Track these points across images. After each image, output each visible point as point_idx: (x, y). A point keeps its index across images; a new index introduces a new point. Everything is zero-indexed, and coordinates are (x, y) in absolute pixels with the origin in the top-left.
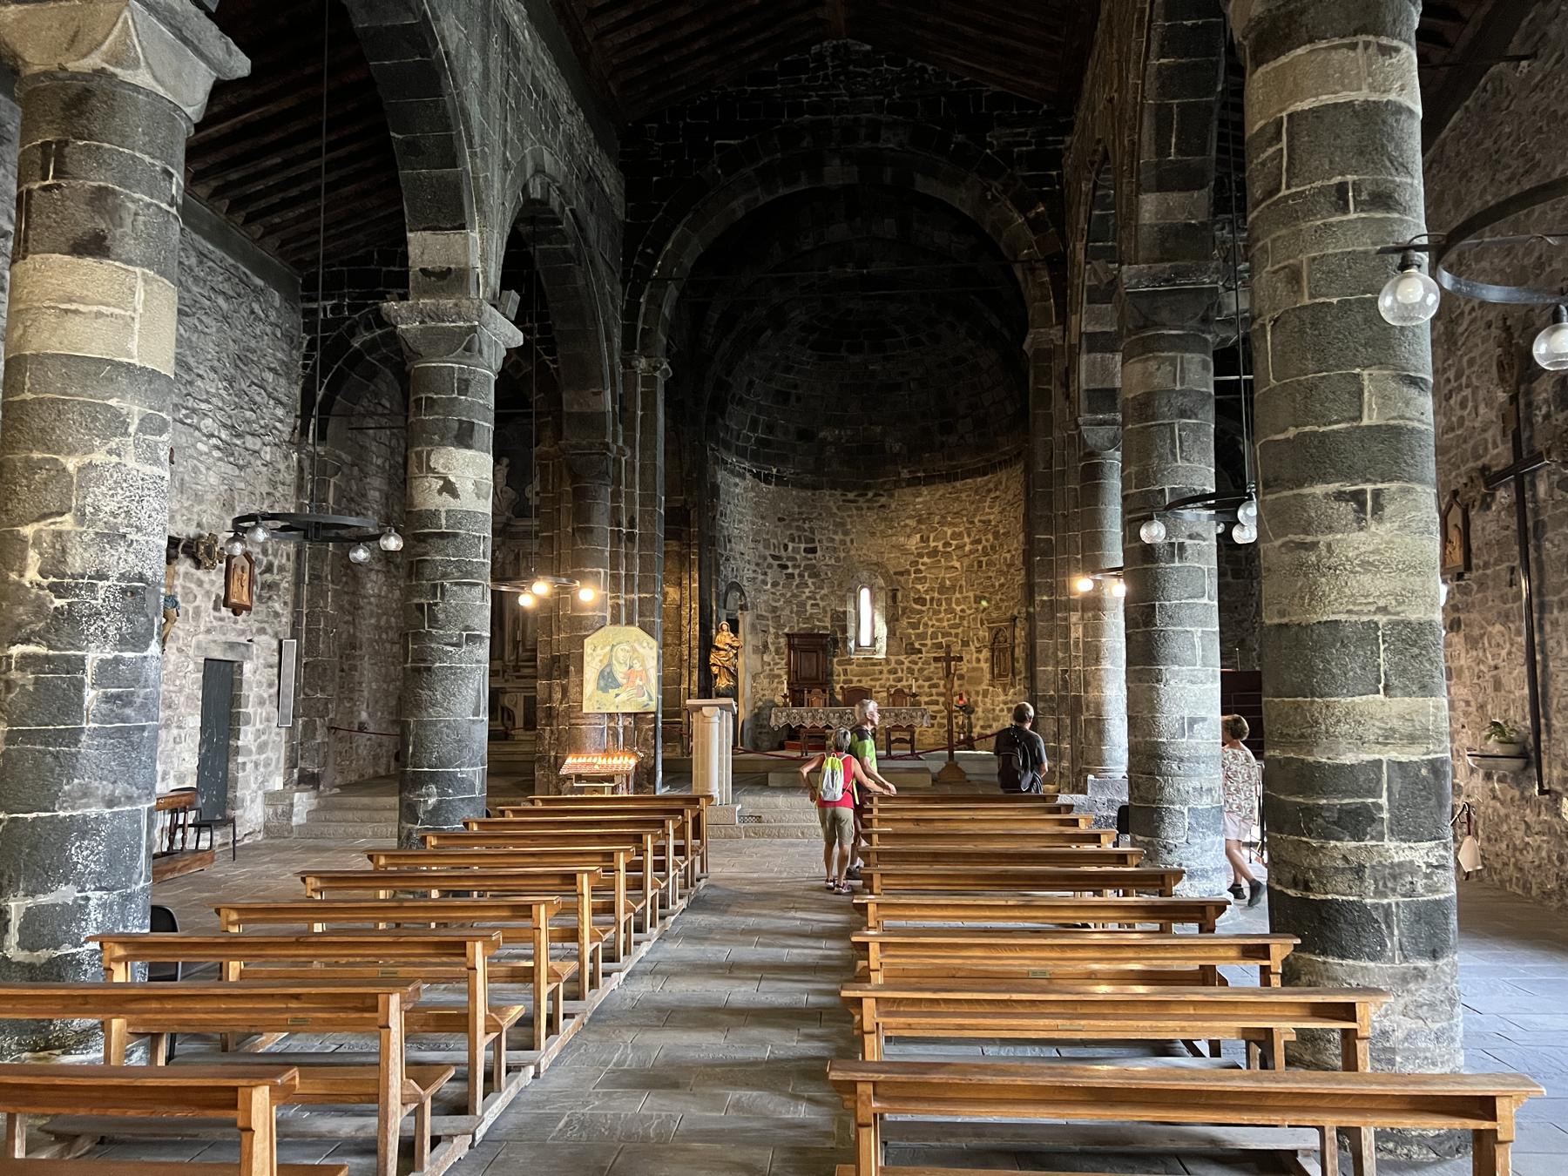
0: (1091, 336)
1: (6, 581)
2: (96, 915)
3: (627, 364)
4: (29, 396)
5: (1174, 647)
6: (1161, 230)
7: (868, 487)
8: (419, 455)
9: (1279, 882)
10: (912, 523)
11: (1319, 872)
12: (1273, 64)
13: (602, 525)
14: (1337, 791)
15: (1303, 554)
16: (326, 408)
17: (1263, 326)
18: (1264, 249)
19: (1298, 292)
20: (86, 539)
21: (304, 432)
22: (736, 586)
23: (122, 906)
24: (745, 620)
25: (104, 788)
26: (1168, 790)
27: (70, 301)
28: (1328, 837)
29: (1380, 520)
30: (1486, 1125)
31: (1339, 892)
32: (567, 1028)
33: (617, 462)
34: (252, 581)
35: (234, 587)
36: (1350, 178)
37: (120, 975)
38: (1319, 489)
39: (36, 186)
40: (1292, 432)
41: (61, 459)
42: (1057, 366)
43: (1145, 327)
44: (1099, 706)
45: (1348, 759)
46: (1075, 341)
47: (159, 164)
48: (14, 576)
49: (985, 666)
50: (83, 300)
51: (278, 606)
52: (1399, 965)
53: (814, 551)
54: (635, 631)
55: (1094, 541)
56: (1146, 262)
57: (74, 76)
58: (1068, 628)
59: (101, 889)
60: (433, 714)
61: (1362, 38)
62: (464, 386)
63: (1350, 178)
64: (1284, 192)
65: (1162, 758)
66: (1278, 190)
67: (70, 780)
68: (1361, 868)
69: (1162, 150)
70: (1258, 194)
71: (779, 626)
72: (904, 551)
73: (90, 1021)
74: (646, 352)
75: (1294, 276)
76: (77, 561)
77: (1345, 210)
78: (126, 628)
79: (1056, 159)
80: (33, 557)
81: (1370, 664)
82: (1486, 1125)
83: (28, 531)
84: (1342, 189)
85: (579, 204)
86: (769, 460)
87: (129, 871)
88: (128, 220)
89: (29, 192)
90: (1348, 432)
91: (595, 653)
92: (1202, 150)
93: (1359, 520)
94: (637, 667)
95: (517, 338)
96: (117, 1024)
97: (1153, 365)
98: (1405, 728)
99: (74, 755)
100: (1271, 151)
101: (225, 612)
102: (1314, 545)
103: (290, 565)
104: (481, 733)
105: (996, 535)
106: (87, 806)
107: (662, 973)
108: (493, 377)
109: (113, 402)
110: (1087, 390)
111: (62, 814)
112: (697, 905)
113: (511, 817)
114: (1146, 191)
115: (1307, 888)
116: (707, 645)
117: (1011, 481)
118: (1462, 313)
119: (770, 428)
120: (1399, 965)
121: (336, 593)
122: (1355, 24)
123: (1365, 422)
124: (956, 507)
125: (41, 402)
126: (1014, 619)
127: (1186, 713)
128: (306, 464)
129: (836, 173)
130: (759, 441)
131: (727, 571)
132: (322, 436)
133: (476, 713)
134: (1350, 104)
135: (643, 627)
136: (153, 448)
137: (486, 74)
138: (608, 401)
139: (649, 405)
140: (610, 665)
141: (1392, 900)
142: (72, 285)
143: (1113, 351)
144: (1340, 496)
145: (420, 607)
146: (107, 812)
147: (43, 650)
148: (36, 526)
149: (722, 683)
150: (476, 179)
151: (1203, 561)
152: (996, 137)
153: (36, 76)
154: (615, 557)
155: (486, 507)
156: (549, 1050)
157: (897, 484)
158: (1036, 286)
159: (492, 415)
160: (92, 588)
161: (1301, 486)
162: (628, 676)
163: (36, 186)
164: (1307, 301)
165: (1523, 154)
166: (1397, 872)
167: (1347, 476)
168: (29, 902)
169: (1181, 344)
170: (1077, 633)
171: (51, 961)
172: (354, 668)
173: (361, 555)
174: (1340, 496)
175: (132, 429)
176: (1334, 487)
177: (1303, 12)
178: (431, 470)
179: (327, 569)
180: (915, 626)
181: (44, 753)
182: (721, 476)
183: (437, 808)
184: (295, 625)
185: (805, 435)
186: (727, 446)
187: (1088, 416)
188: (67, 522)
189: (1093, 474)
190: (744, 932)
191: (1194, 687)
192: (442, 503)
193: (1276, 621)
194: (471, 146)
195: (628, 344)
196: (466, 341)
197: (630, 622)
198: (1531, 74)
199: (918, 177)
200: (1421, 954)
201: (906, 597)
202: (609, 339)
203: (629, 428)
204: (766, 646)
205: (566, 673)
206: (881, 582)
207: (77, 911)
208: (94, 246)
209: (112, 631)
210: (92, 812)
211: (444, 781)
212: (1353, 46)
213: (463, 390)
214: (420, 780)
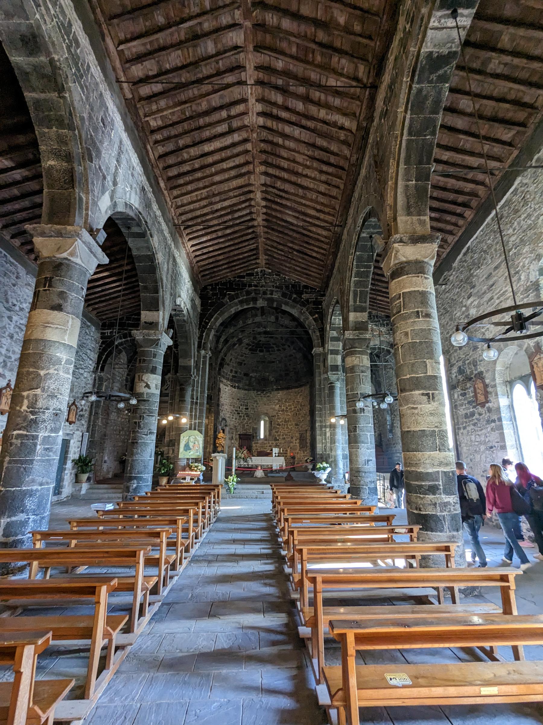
0: (331, 350)
1: (15, 410)
2: (31, 524)
3: (198, 351)
4: (31, 351)
5: (362, 439)
6: (355, 322)
7: (264, 390)
8: (139, 376)
9: (411, 508)
10: (277, 401)
11: (424, 505)
13: (188, 399)
15: (413, 410)
16: (105, 361)
18: (397, 327)
19: (408, 338)
20: (44, 397)
21: (97, 368)
22: (224, 419)
23: (41, 521)
24: (227, 429)
25: (40, 479)
26: (362, 482)
27: (48, 323)
28: (426, 494)
29: (434, 401)
30: (506, 584)
31: (430, 511)
32: (185, 562)
33: (194, 380)
34: (76, 414)
35: (71, 416)
36: (419, 309)
37: (38, 545)
38: (417, 392)
39: (41, 289)
40: (408, 376)
41: (39, 371)
45: (430, 471)
47: (80, 286)
48: (18, 408)
49: (298, 445)
50: (52, 323)
51: (83, 422)
52: (448, 534)
53: (247, 409)
54: (196, 432)
55: (333, 408)
57: (58, 258)
58: (326, 433)
59: (34, 515)
60: (137, 457)
61: (420, 275)
62: (155, 356)
63: (419, 309)
64: (402, 312)
67: (28, 476)
68: (436, 503)
69: (355, 301)
71: (237, 432)
72: (274, 409)
73: (25, 563)
74: (204, 348)
75: (406, 334)
76: (40, 404)
77: (419, 317)
78: (53, 425)
79: (320, 303)
80: (26, 402)
81: (434, 442)
82: (506, 584)
83: (25, 394)
85: (189, 306)
86: (235, 381)
87: (44, 508)
88: (69, 301)
89: (39, 291)
90: (424, 377)
91: (184, 439)
92: (365, 302)
93: (429, 401)
94: (196, 443)
95: (171, 343)
96: (35, 563)
97: (354, 358)
98: (445, 461)
99: (31, 468)
101: (67, 424)
102: (416, 408)
103: (88, 409)
104: (151, 464)
105: (301, 405)
106: (33, 486)
107: (212, 543)
108: (163, 353)
109: (58, 354)
111: (24, 488)
112: (218, 520)
113: (159, 491)
115: (420, 510)
116: (216, 437)
117: (305, 390)
119: (236, 372)
120: (448, 534)
121: (102, 419)
122: (418, 271)
123: (428, 374)
124: (290, 397)
125: (35, 353)
126: (306, 431)
127: (366, 458)
128: (97, 378)
129: (261, 303)
130: (233, 376)
131: (221, 414)
132: (102, 370)
133: (151, 457)
134: (418, 291)
135: (199, 431)
136: (68, 369)
137: (168, 269)
138: (192, 363)
139: (204, 363)
140: (188, 442)
141: (445, 513)
142: (49, 319)
143: (337, 355)
144: (423, 394)
145: (135, 423)
146: (39, 488)
147: (25, 433)
148: (28, 392)
149: (220, 449)
150: (163, 297)
151: (369, 414)
152: (305, 296)
153: (46, 258)
154: (191, 408)
155: (158, 392)
156: (180, 569)
157: (273, 390)
158: (315, 336)
159: (162, 365)
160: (44, 412)
161: (411, 391)
162: (193, 447)
163: (41, 289)
164: (410, 341)
165: (444, 309)
166: (446, 504)
167: (424, 388)
168: (9, 520)
170: (328, 434)
171: (14, 541)
172: (105, 442)
173: (122, 405)
174: (423, 394)
175: (63, 363)
176: (421, 392)
177: (405, 267)
178: (142, 380)
179: (100, 411)
180: (277, 432)
181: (20, 467)
182: (222, 386)
183: (136, 488)
184: (88, 428)
185: (246, 375)
186: (224, 377)
188: (38, 391)
189: (332, 388)
190: (235, 529)
192: (145, 390)
193: (406, 430)
194: (162, 288)
195: (199, 347)
196: (156, 342)
197: (195, 429)
198: (445, 289)
199: (283, 305)
200: (454, 530)
201: (274, 423)
202: (194, 345)
203: (198, 370)
204: (232, 438)
205: (174, 445)
206: (267, 419)
207: (24, 523)
208: (58, 308)
209: (49, 427)
210: (35, 488)
211: (139, 479)
212: (418, 277)
213: (154, 357)
214: (131, 479)
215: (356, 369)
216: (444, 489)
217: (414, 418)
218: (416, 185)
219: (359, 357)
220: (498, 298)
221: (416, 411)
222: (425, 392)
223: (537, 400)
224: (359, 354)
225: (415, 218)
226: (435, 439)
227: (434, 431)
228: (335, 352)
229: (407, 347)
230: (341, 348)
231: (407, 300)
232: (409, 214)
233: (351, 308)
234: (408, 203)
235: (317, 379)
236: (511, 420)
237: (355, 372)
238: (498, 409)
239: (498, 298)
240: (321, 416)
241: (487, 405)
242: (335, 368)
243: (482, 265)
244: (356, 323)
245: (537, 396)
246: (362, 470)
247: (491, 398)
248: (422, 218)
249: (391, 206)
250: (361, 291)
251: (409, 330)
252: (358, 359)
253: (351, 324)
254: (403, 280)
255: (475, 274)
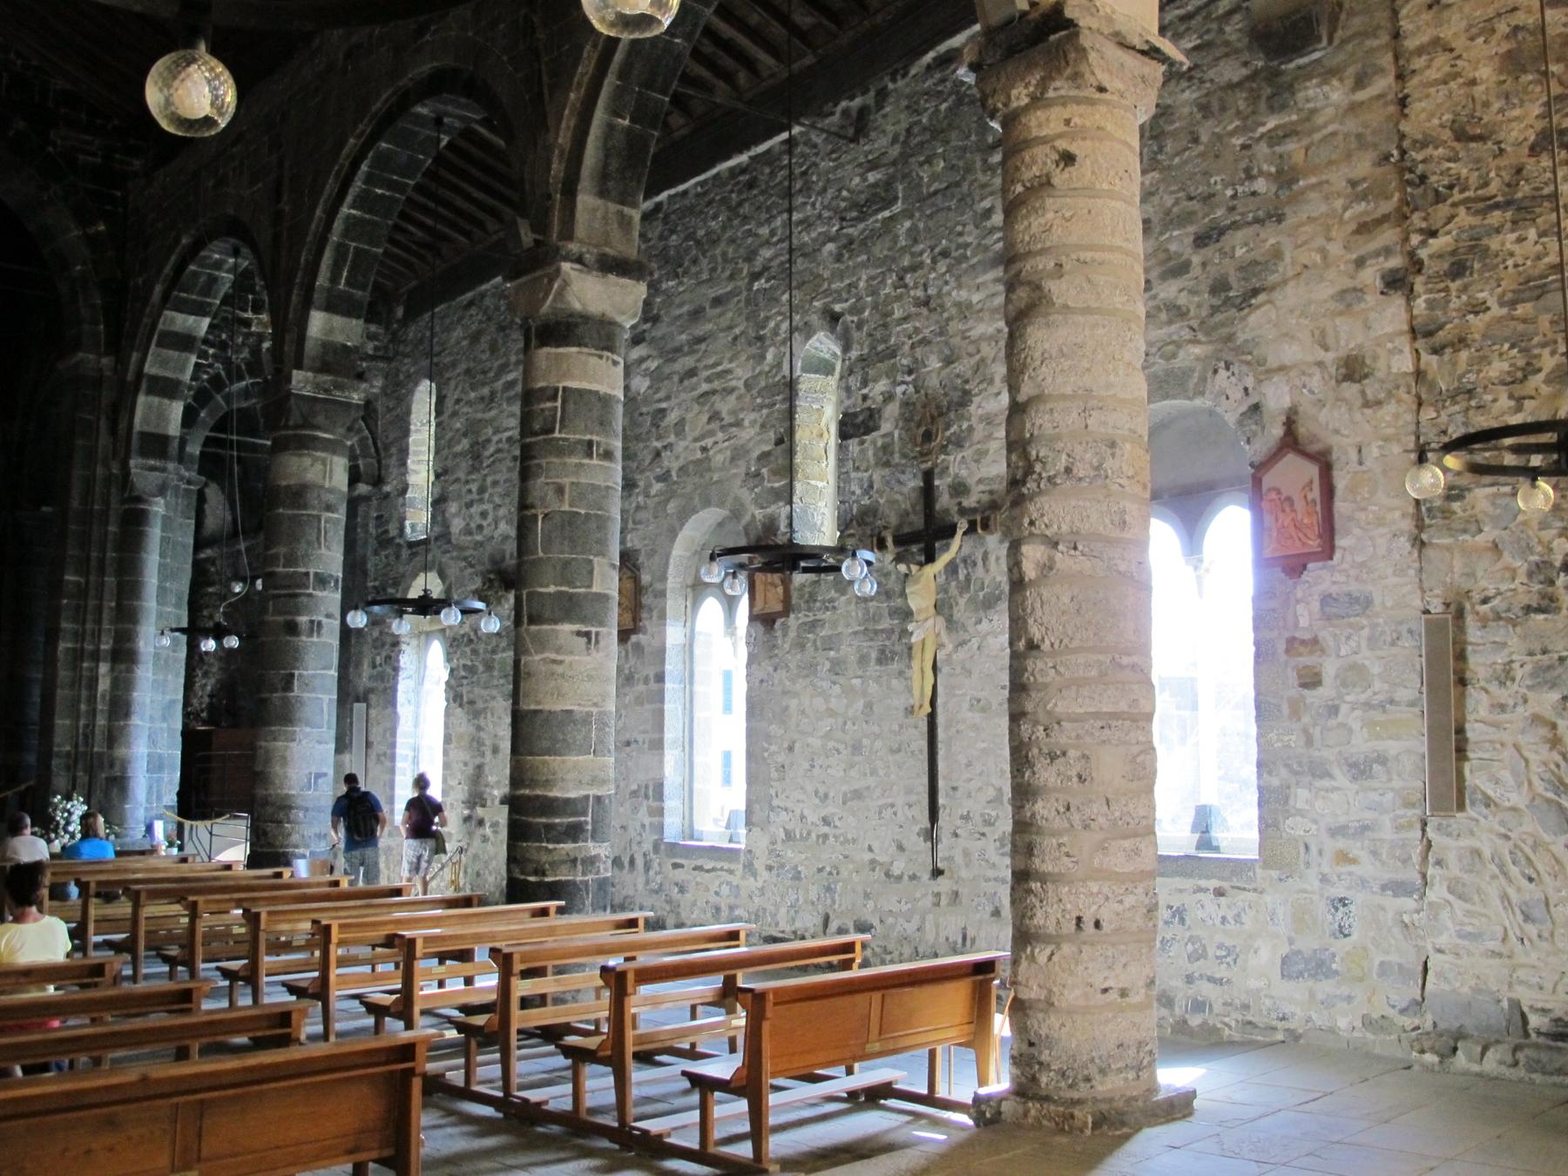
5: (307, 712)
12: (553, 350)
14: (564, 814)
17: (536, 516)
18: (540, 466)
19: (562, 501)
26: (295, 838)
36: (595, 438)
38: (567, 628)
40: (552, 589)
42: (107, 396)
43: (303, 427)
44: (124, 764)
45: (572, 795)
46: (130, 377)
56: (310, 369)
58: (94, 681)
61: (606, 353)
64: (556, 435)
65: (290, 808)
66: (552, 431)
69: (334, 279)
70: (537, 427)
77: (590, 455)
84: (590, 443)
90: (586, 595)
97: (307, 461)
100: (549, 405)
102: (561, 662)
110: (143, 434)
114: (319, 309)
115: (544, 874)
118: (488, 441)
127: (314, 769)
134: (597, 393)
141: (589, 877)
144: (579, 633)
161: (555, 622)
164: (566, 508)
167: (583, 620)
169: (332, 447)
170: (104, 685)
174: (579, 633)
176: (576, 627)
187: (140, 461)
189: (134, 521)
191: (321, 747)
193: (533, 707)
212: (601, 357)
215: (312, 498)
216: (594, 831)
217: (552, 684)
218: (628, 131)
219: (324, 464)
220: (709, 380)
221: (559, 669)
222: (584, 629)
223: (748, 643)
224: (324, 449)
225: (613, 207)
226: (590, 731)
227: (589, 714)
228: (166, 388)
229: (558, 518)
230: (187, 376)
231: (571, 407)
232: (603, 193)
233: (317, 297)
234: (605, 165)
235: (78, 473)
236: (682, 681)
237: (305, 507)
238: (661, 653)
239: (709, 380)
240: (79, 615)
241: (634, 638)
242: (156, 445)
243: (686, 273)
244: (327, 346)
245: (749, 635)
246: (299, 802)
247: (648, 623)
248: (626, 210)
249: (562, 152)
250: (357, 251)
251: (566, 481)
252: (319, 466)
253: (310, 347)
254: (567, 356)
255: (664, 286)
